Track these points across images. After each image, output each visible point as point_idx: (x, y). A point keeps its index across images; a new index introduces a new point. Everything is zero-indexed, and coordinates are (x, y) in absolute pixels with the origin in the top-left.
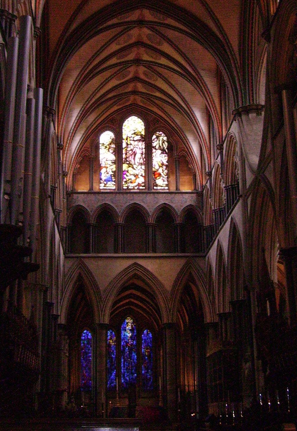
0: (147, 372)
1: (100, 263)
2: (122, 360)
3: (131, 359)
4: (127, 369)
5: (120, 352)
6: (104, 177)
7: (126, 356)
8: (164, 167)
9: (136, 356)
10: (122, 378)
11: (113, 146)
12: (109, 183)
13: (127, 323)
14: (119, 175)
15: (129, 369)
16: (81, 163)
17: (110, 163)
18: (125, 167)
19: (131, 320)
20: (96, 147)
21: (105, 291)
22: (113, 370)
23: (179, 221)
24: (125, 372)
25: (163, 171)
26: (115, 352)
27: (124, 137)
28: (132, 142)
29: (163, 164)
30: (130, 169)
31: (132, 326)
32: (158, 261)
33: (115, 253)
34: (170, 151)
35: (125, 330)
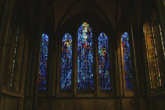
0: (104, 72)
2: (78, 61)
3: (88, 60)
4: (83, 69)
7: (83, 57)
10: (78, 79)
13: (84, 27)
15: (86, 69)
22: (68, 70)
26: (71, 53)
31: (88, 30)
35: (82, 33)
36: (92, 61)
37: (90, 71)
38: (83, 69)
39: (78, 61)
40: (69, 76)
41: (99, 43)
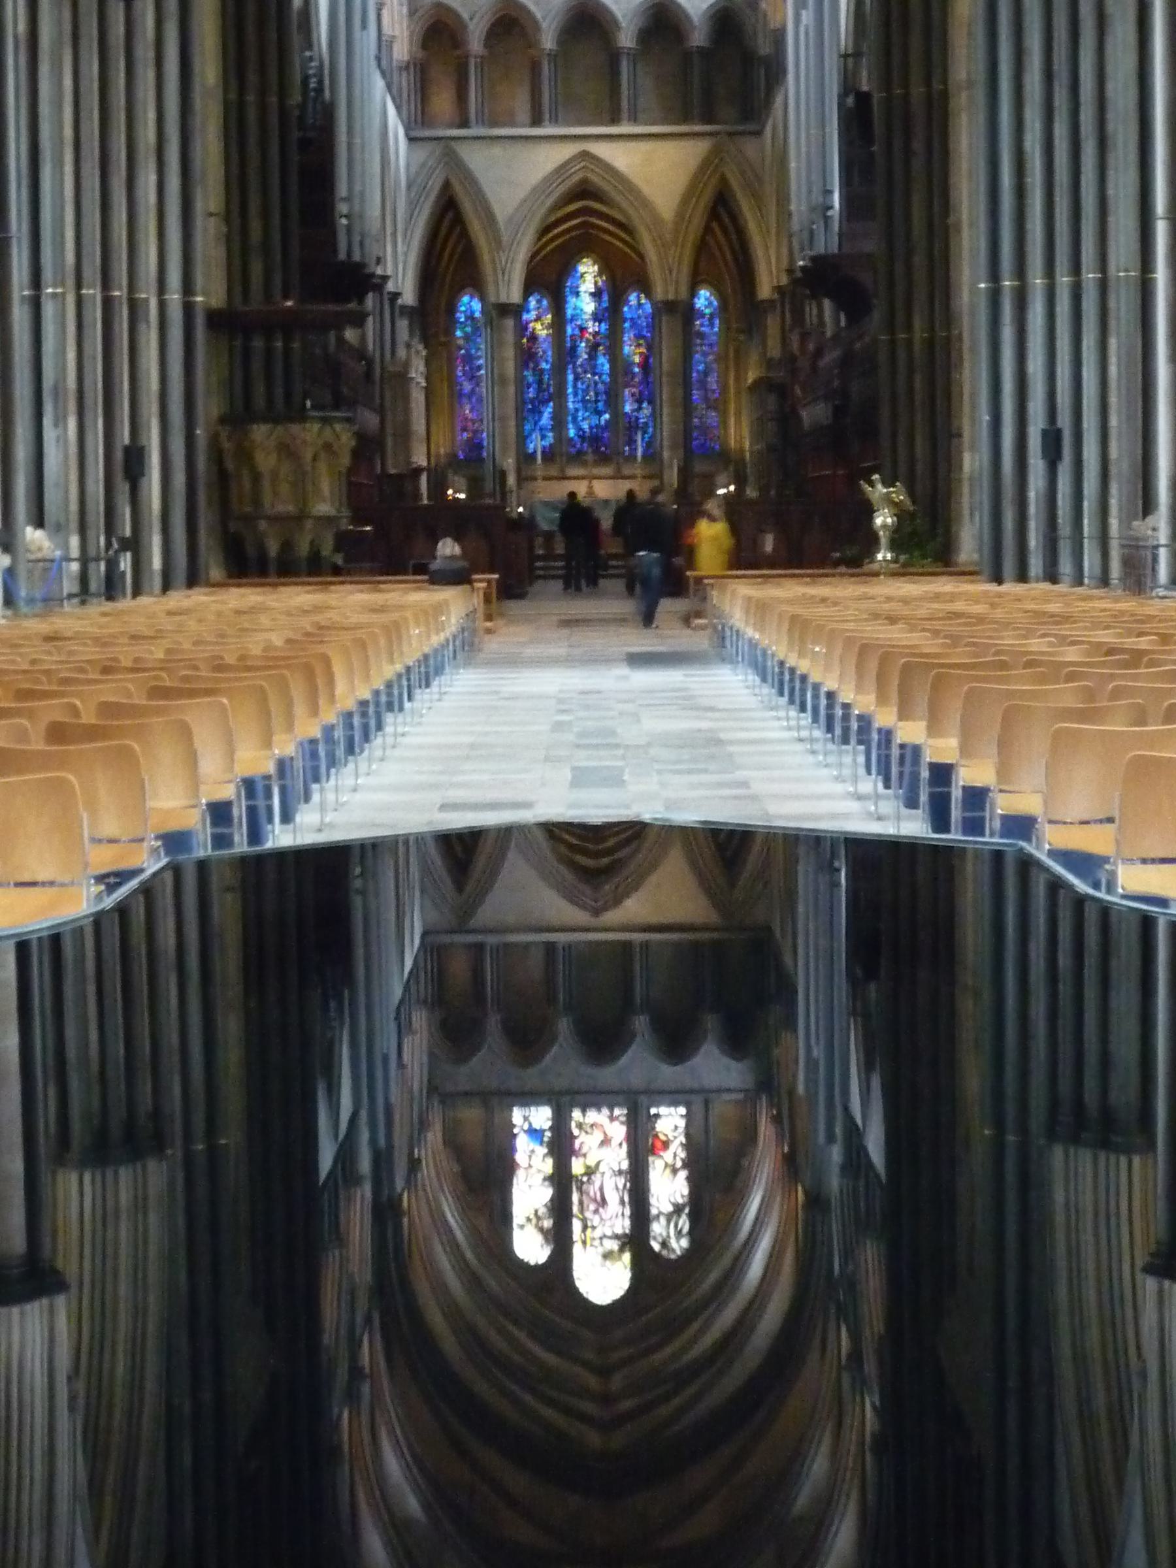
0: (640, 408)
1: (497, 150)
2: (571, 377)
3: (594, 374)
5: (565, 354)
7: (581, 366)
9: (607, 367)
13: (582, 276)
15: (589, 401)
19: (594, 265)
21: (510, 220)
22: (545, 402)
23: (698, 38)
24: (577, 410)
26: (550, 353)
31: (596, 283)
32: (644, 146)
35: (577, 294)
36: (606, 378)
37: (600, 405)
38: (583, 401)
39: (571, 377)
40: (546, 419)
41: (627, 325)
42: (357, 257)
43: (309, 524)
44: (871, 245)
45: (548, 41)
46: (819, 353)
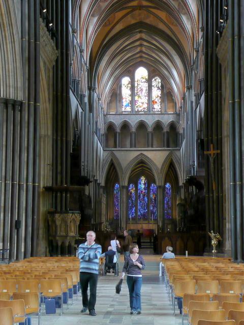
0: (154, 209)
6: (124, 104)
8: (159, 98)
11: (130, 85)
12: (127, 107)
14: (133, 103)
16: (111, 96)
17: (128, 96)
18: (136, 98)
20: (120, 87)
23: (166, 129)
25: (158, 100)
27: (136, 80)
28: (140, 83)
29: (158, 96)
30: (139, 99)
32: (154, 152)
33: (131, 147)
34: (162, 88)
40: (133, 211)
42: (86, 175)
43: (68, 238)
44: (204, 174)
45: (134, 130)
46: (192, 198)
